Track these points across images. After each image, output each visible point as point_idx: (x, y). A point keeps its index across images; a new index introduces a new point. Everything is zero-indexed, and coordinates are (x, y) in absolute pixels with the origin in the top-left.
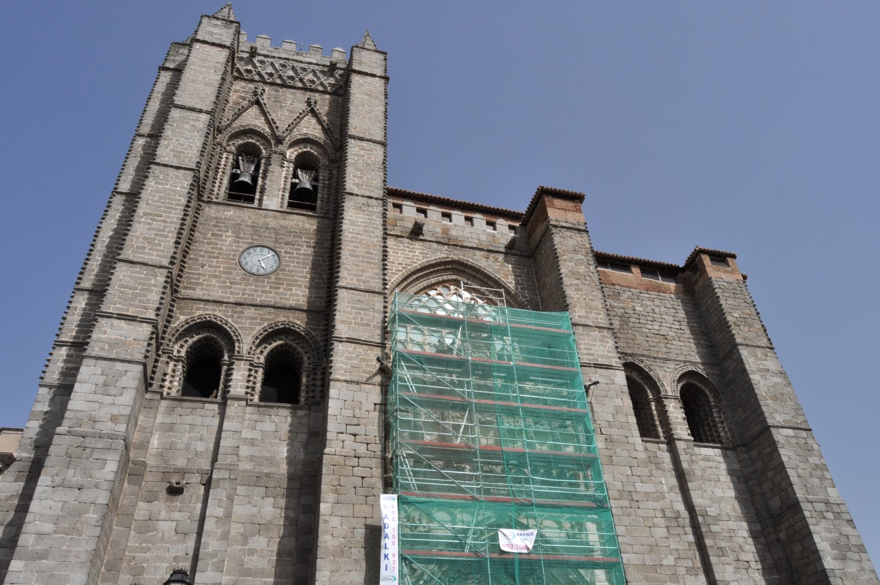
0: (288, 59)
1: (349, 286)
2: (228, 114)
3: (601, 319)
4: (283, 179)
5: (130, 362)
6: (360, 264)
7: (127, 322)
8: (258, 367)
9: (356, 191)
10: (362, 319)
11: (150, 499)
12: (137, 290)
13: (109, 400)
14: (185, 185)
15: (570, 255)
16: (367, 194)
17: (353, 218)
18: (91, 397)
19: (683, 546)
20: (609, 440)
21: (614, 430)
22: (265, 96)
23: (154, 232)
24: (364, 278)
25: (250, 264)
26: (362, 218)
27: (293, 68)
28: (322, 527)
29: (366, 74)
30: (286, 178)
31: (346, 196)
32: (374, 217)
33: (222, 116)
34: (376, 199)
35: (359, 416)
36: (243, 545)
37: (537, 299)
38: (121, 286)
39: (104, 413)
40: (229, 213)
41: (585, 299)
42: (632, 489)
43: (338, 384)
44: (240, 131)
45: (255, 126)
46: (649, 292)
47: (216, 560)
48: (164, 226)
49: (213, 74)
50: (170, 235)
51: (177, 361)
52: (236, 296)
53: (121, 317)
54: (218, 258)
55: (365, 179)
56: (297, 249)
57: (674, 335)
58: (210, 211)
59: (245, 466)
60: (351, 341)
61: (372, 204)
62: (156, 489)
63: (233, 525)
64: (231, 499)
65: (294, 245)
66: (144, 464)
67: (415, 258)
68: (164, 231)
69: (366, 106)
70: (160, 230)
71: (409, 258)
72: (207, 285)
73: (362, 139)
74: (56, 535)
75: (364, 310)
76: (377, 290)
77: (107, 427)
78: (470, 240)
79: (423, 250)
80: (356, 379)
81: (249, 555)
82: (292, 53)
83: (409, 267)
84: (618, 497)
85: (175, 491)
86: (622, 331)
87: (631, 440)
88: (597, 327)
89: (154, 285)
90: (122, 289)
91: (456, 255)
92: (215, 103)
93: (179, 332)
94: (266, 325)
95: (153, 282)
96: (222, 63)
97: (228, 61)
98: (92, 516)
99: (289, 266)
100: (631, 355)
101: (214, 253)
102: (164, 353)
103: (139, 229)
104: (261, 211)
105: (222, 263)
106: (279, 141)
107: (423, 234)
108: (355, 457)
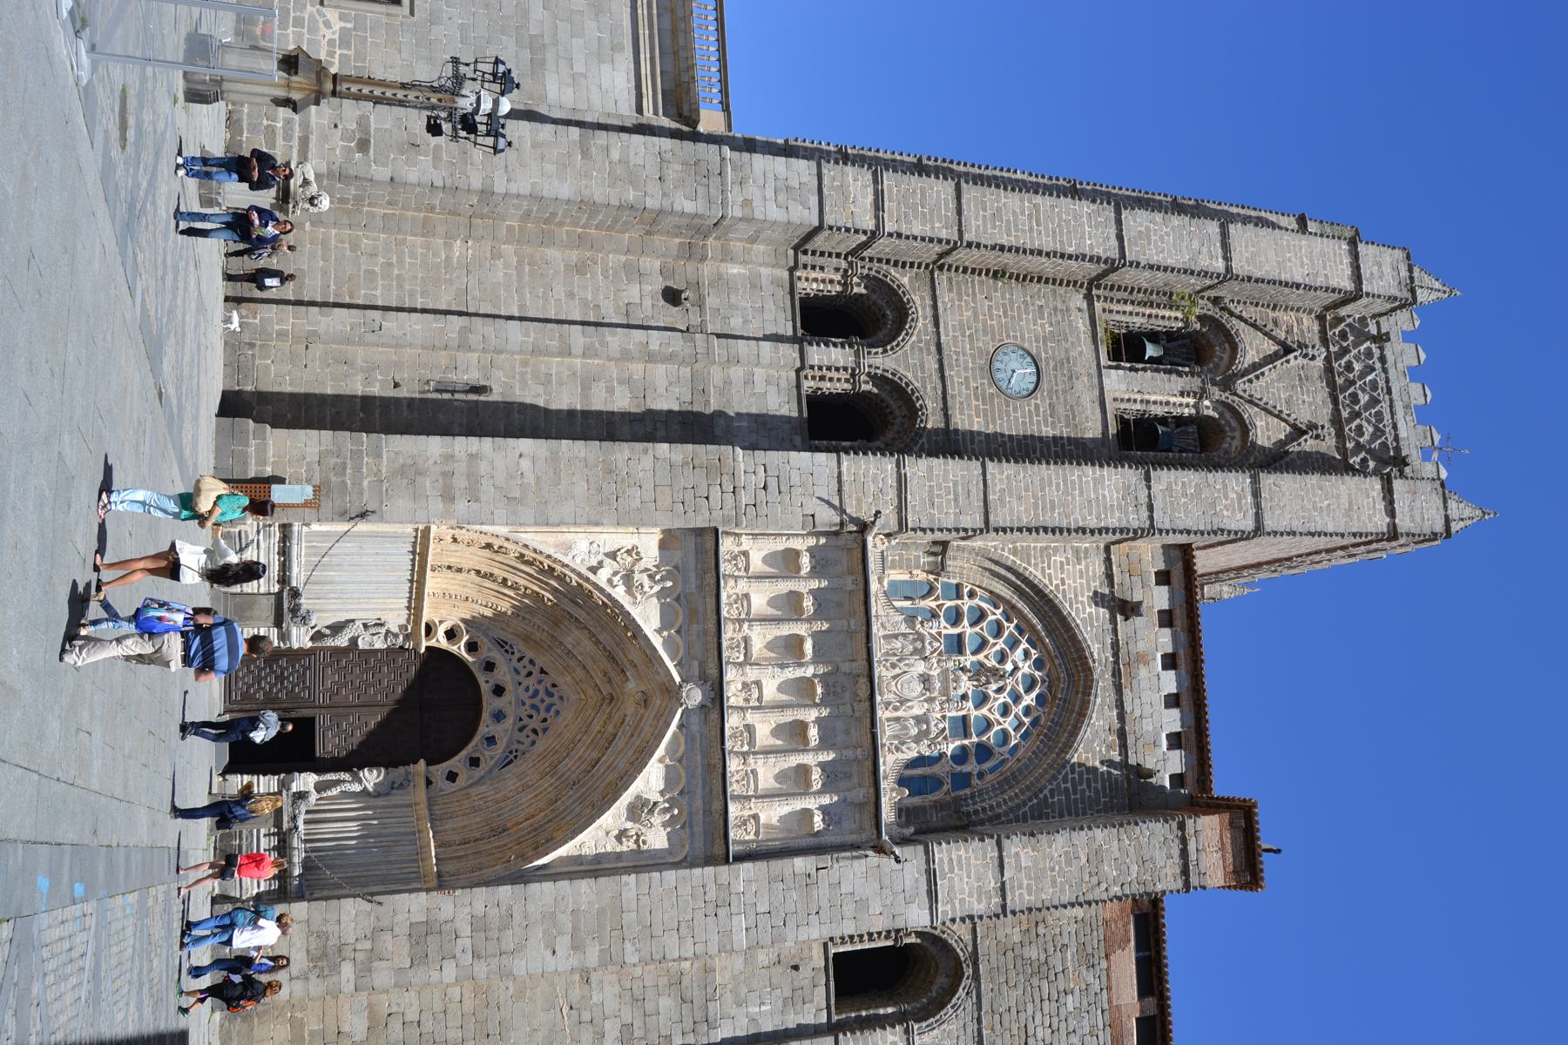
0: (1389, 391)
1: (989, 477)
2: (1250, 312)
3: (1021, 894)
4: (1164, 398)
10: (939, 496)
13: (770, 193)
15: (1132, 850)
16: (1157, 505)
18: (770, 176)
21: (827, 891)
25: (1006, 358)
26: (1111, 497)
27: (1374, 401)
28: (639, 446)
30: (1167, 403)
33: (1245, 303)
34: (1151, 518)
38: (923, 190)
39: (752, 190)
42: (734, 909)
48: (1024, 231)
54: (1005, 313)
56: (1046, 421)
58: (1078, 300)
59: (716, 374)
60: (901, 482)
63: (641, 366)
64: (670, 358)
66: (703, 259)
70: (1016, 226)
71: (1076, 596)
73: (1256, 494)
75: (956, 500)
76: (991, 518)
77: (735, 196)
78: (1137, 701)
80: (846, 488)
82: (1405, 398)
84: (719, 882)
86: (1019, 962)
87: (814, 919)
89: (933, 228)
94: (916, 384)
96: (1327, 282)
97: (1334, 290)
98: (631, 195)
99: (1015, 410)
103: (1011, 201)
105: (1000, 324)
106: (1227, 384)
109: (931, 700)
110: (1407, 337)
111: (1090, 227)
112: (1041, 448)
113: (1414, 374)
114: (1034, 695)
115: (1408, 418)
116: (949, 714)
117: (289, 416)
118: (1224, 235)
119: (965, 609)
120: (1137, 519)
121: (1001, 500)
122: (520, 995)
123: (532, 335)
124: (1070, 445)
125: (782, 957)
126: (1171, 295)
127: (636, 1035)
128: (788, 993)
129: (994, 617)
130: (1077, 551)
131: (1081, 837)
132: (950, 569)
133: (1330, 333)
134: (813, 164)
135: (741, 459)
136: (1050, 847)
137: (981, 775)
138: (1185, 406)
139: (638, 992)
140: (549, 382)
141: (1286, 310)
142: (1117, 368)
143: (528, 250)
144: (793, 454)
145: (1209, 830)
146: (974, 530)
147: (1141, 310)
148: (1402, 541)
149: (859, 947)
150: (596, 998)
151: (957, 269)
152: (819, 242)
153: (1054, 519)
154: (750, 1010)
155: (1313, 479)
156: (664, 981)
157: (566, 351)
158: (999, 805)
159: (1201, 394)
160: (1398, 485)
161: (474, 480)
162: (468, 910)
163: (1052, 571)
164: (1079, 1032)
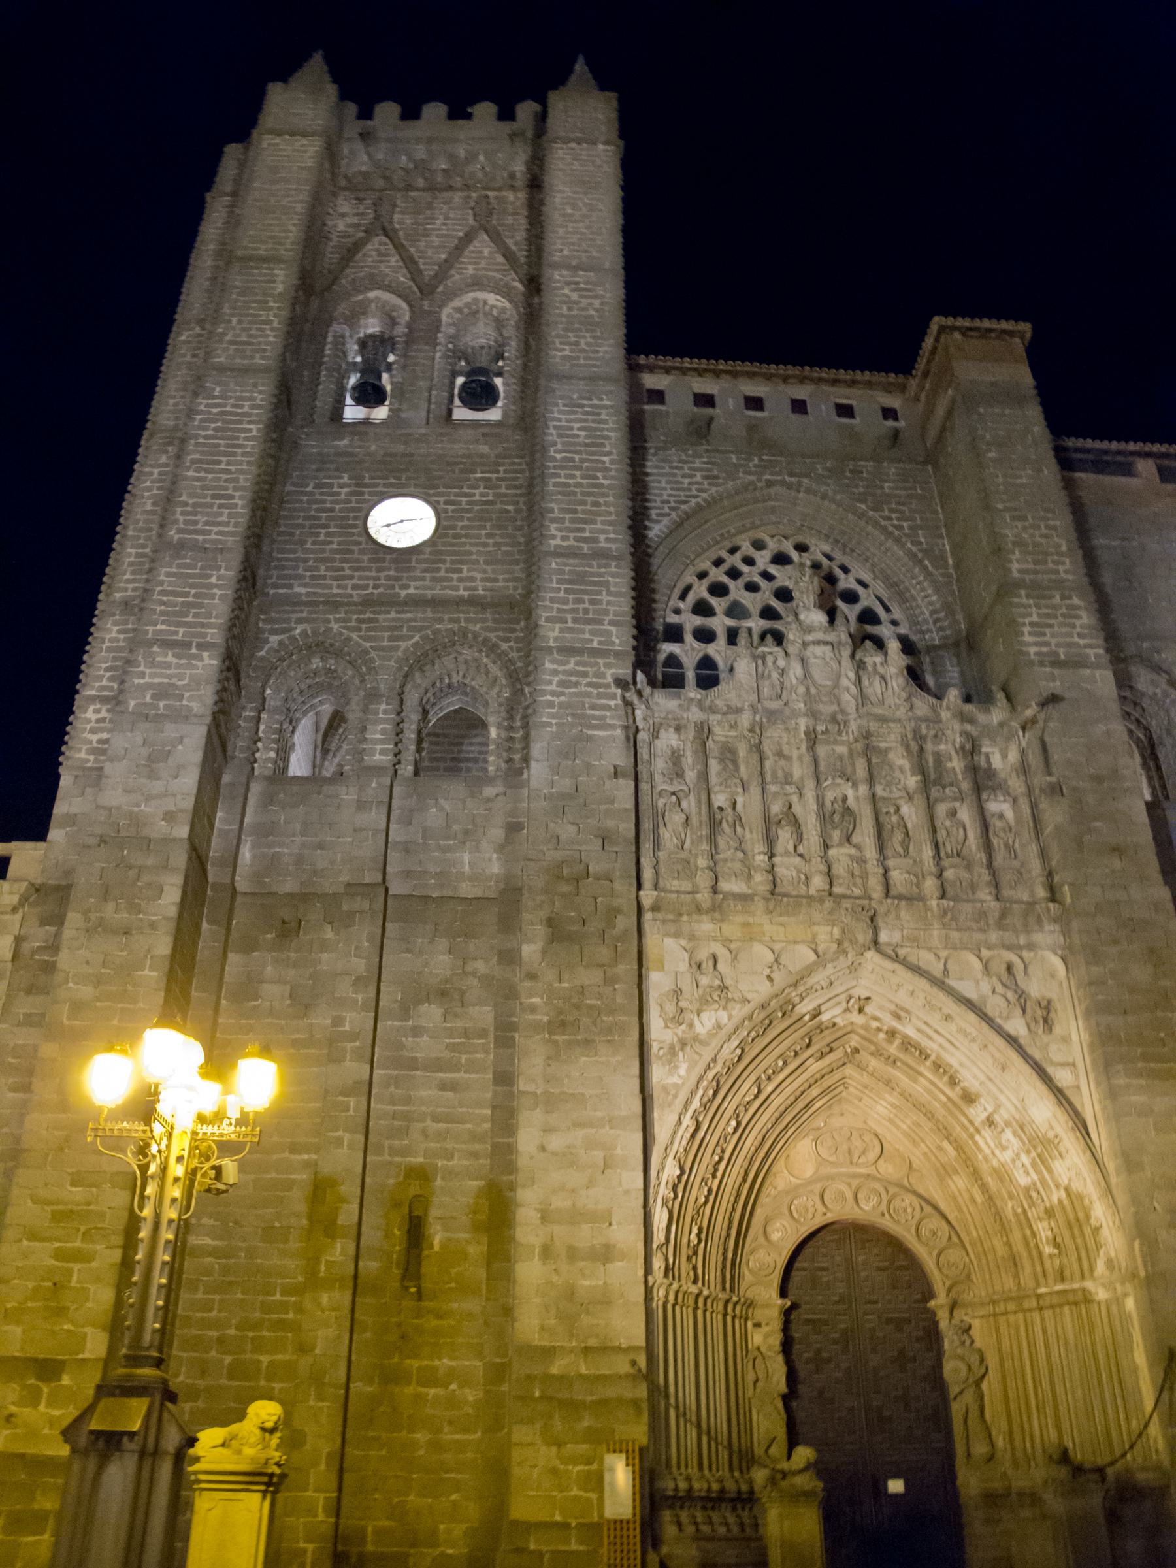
3: (1066, 572)
6: (579, 508)
11: (249, 946)
13: (157, 786)
14: (258, 402)
24: (587, 534)
26: (580, 421)
32: (603, 417)
41: (1032, 536)
47: (357, 1044)
50: (237, 494)
53: (168, 645)
54: (326, 526)
56: (466, 495)
60: (568, 651)
67: (694, 488)
72: (312, 577)
74: (98, 1004)
81: (415, 1036)
89: (216, 586)
90: (165, 599)
94: (417, 638)
95: (213, 580)
99: (454, 527)
101: (319, 518)
111: (225, 406)
112: (502, 503)
117: (454, 1497)
121: (585, 540)
123: (340, 1133)
137: (895, 623)
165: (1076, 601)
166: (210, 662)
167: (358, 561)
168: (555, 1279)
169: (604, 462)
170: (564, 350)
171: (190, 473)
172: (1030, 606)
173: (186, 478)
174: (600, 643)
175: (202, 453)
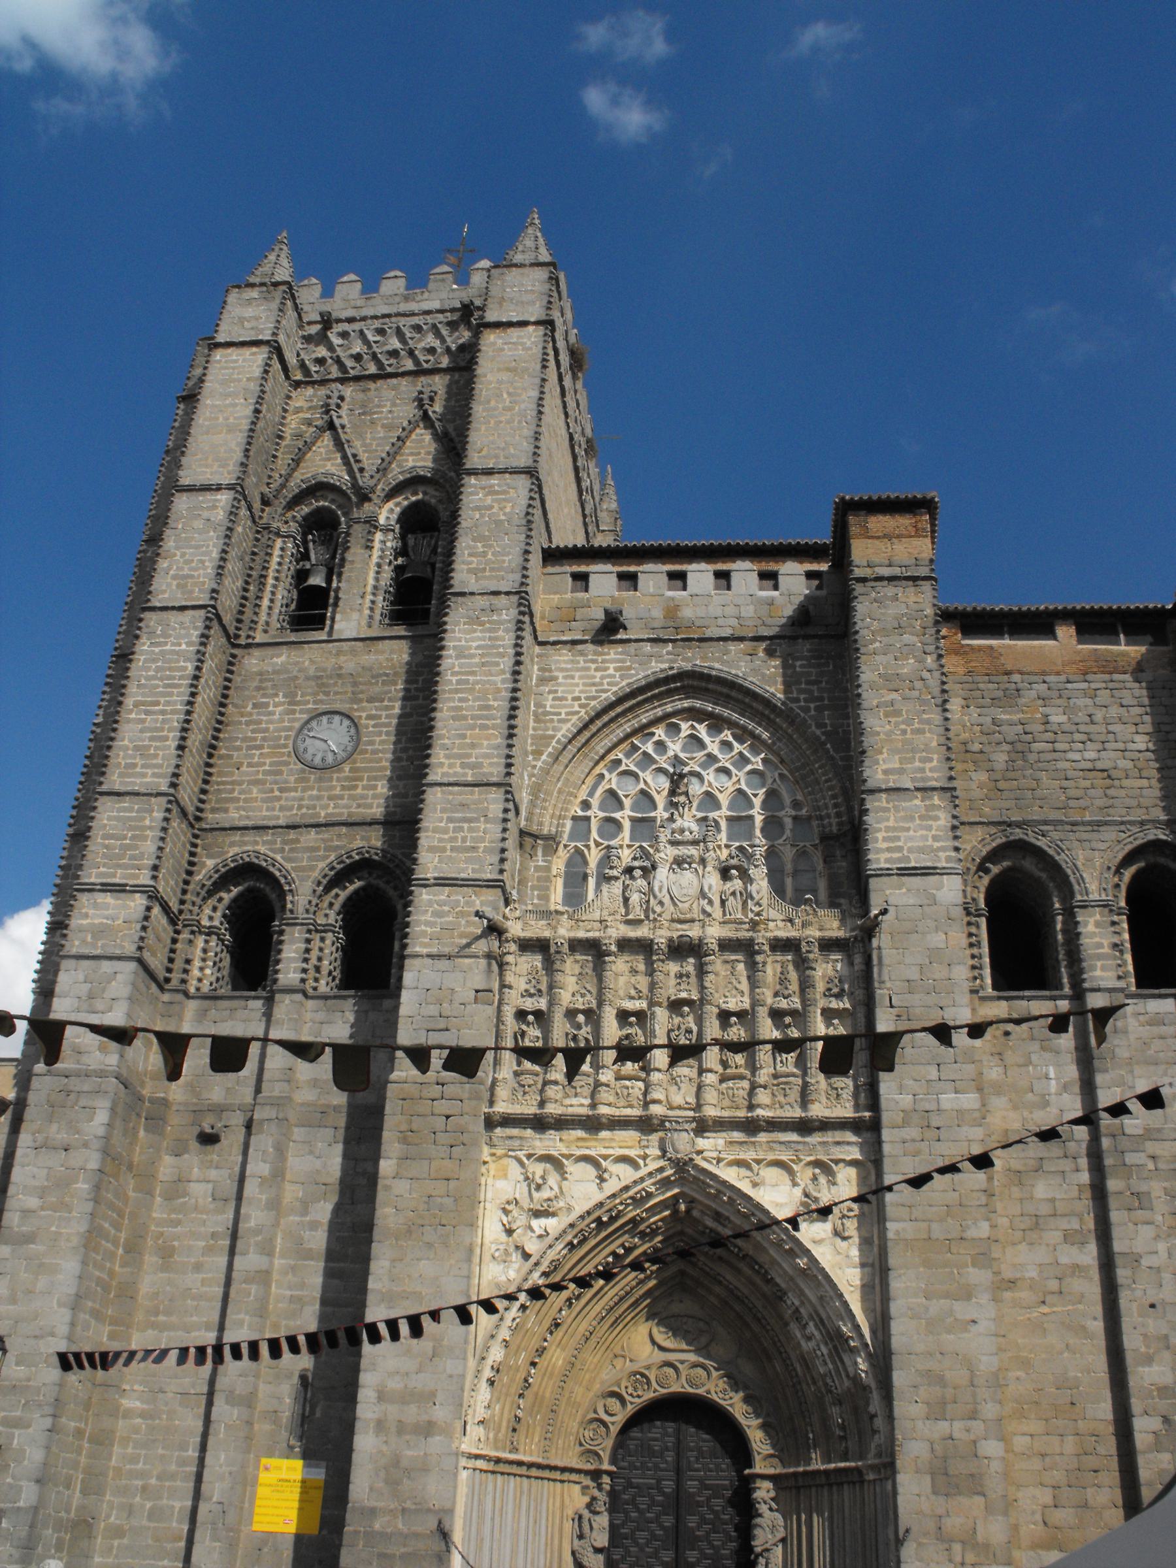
0: (389, 316)
1: (445, 780)
3: (931, 770)
4: (373, 569)
5: (119, 958)
7: (115, 894)
8: (325, 931)
9: (472, 584)
10: (464, 840)
12: (125, 838)
14: (194, 639)
15: (885, 640)
17: (463, 643)
19: (1066, 1193)
20: (904, 1017)
21: (917, 996)
22: (344, 412)
23: (149, 734)
25: (311, 751)
28: (381, 1195)
29: (510, 324)
30: (379, 565)
31: (453, 599)
32: (501, 633)
34: (507, 593)
35: (449, 1014)
36: (302, 1215)
37: (848, 725)
38: (107, 837)
40: (279, 660)
42: (933, 1107)
43: (417, 962)
44: (302, 492)
45: (325, 474)
46: (1090, 677)
47: (260, 1238)
48: (164, 721)
49: (242, 404)
50: (171, 735)
51: (208, 934)
52: (288, 814)
53: (108, 888)
54: (261, 747)
55: (490, 556)
56: (387, 708)
57: (1130, 765)
58: (252, 662)
60: (443, 882)
61: (499, 606)
62: (185, 1136)
63: (288, 1187)
65: (382, 701)
67: (605, 681)
68: (162, 730)
69: (505, 396)
70: (157, 729)
71: (594, 684)
72: (246, 800)
73: (489, 472)
74: (43, 1213)
76: (494, 779)
78: (720, 622)
79: (623, 661)
80: (446, 950)
81: (311, 1229)
82: (397, 299)
83: (593, 703)
85: (209, 1139)
86: (1011, 775)
88: (918, 789)
89: (150, 828)
91: (684, 659)
92: (242, 464)
93: (206, 889)
94: (332, 858)
95: (147, 822)
98: (83, 1186)
99: (372, 743)
100: (1018, 825)
101: (255, 739)
102: (185, 926)
103: (128, 736)
104: (331, 645)
106: (364, 497)
107: (625, 628)
108: (438, 1084)
109: (703, 861)
110: (328, 293)
111: (166, 644)
113: (370, 287)
114: (707, 739)
115: (419, 298)
116: (724, 841)
118: (190, 489)
119: (601, 814)
120: (507, 613)
121: (473, 766)
122: (1026, 1364)
123: (241, 1316)
124: (416, 682)
125: (994, 1050)
126: (254, 553)
127: (1077, 1227)
128: (1036, 1046)
129: (614, 780)
130: (542, 681)
131: (870, 698)
132: (554, 830)
133: (316, 377)
134: (65, 964)
135: (404, 1074)
136: (878, 734)
137: (796, 805)
138: (384, 544)
139: (1028, 1222)
140: (299, 1299)
141: (282, 424)
142: (333, 619)
143: (140, 1316)
144: (403, 1011)
145: (863, 552)
146: (507, 800)
147: (269, 588)
148: (556, 315)
149: (987, 960)
150: (1032, 1273)
151: (202, 801)
152: (157, 963)
153: (500, 705)
154: (1053, 1090)
155: (478, 410)
156: (1016, 1192)
157: (263, 1277)
158: (831, 788)
159: (371, 523)
160: (491, 316)
161: (408, 1397)
162: (920, 1424)
163: (563, 711)
164: (1091, 710)
165: (936, 801)
166: (139, 902)
167: (286, 782)
168: (384, 1448)
169: (495, 683)
170: (470, 563)
171: (133, 716)
172: (887, 810)
173: (129, 721)
174: (474, 871)
175: (143, 695)
